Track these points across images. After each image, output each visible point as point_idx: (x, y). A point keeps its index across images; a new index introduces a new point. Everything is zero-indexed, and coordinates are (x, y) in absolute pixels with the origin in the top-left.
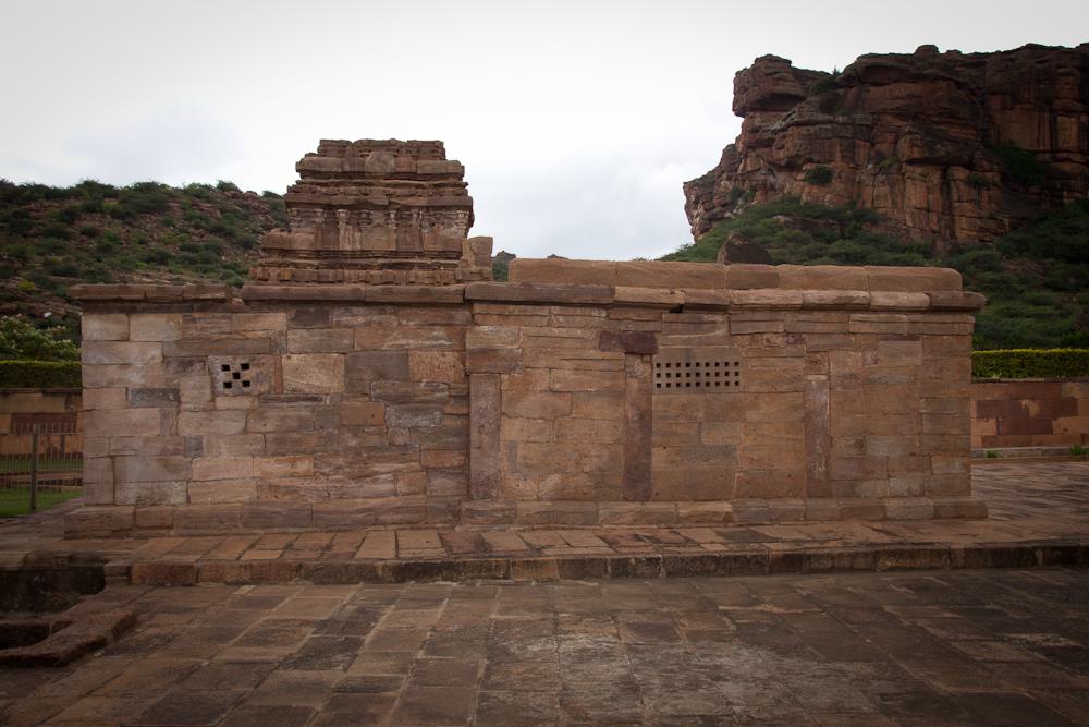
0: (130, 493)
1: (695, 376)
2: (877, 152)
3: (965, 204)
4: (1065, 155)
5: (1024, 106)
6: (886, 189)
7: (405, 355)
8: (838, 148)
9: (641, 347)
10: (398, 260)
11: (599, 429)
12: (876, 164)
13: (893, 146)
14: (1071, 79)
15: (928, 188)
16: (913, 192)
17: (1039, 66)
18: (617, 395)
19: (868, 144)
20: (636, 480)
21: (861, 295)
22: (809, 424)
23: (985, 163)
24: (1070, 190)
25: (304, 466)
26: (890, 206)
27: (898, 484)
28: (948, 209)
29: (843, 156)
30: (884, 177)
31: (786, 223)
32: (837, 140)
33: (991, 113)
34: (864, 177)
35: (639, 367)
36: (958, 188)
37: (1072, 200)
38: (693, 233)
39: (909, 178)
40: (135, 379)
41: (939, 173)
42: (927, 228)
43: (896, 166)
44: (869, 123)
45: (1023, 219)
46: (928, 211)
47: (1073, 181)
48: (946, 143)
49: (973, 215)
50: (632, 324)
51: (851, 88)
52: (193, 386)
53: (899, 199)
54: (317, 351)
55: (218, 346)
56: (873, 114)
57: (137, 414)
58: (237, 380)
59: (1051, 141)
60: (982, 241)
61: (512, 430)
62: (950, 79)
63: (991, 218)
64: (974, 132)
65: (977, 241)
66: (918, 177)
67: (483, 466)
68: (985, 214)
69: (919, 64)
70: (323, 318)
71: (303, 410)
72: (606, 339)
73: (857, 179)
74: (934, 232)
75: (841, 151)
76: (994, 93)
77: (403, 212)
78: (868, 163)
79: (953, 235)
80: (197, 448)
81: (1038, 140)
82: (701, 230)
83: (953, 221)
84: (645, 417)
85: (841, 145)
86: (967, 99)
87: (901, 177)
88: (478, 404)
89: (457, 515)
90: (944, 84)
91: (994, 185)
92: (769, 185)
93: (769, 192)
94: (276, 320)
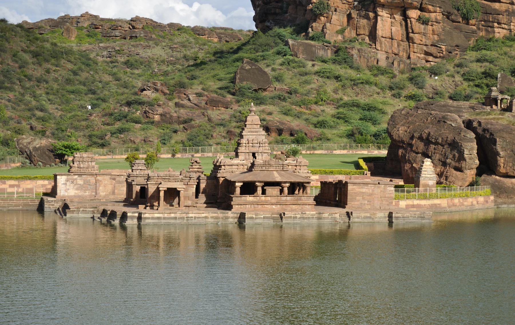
3: (416, 35)
9: (114, 179)
11: (110, 188)
16: (381, 25)
18: (112, 184)
20: (113, 193)
24: (499, 23)
31: (293, 45)
35: (114, 181)
37: (500, 30)
40: (62, 183)
45: (457, 46)
46: (392, 39)
49: (422, 43)
50: (113, 177)
52: (68, 183)
55: (71, 179)
57: (63, 186)
58: (72, 182)
60: (427, 61)
61: (101, 188)
67: (98, 192)
68: (429, 42)
72: (110, 179)
74: (395, 54)
79: (409, 57)
80: (68, 189)
82: (258, 19)
83: (409, 45)
84: (115, 187)
91: (437, 22)
92: (298, 3)
93: (299, 7)
94: (76, 176)
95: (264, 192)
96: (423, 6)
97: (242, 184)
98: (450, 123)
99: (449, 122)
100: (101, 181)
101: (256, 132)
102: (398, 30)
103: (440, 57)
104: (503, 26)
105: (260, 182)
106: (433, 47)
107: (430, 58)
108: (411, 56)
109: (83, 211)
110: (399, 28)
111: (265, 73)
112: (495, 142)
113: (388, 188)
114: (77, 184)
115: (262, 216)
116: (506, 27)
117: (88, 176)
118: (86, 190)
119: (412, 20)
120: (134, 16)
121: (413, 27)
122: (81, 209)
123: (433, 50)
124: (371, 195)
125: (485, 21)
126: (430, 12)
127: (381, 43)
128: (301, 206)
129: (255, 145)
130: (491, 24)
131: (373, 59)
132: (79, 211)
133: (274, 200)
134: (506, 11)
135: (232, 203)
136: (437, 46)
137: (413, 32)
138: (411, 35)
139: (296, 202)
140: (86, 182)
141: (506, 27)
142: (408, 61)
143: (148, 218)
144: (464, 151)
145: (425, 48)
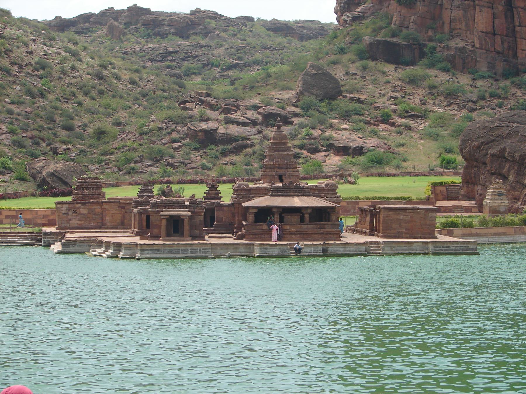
6: (459, 13)
7: (95, 209)
9: (123, 208)
10: (92, 195)
11: (118, 217)
15: (494, 14)
16: (480, 18)
18: (121, 213)
25: (83, 222)
26: (464, 28)
36: (518, 14)
38: (336, 12)
39: (478, 5)
40: (63, 212)
42: (493, 49)
46: (494, 34)
50: (122, 205)
52: (70, 213)
53: (471, 23)
58: (75, 212)
61: (108, 218)
70: (85, 205)
71: (83, 216)
72: (119, 207)
74: (498, 53)
79: (515, 56)
80: (70, 220)
83: (516, 41)
88: (104, 213)
94: (80, 205)
97: (255, 211)
108: (519, 54)
111: (335, 78)
113: (429, 214)
114: (80, 214)
120: (194, 9)
137: (520, 26)
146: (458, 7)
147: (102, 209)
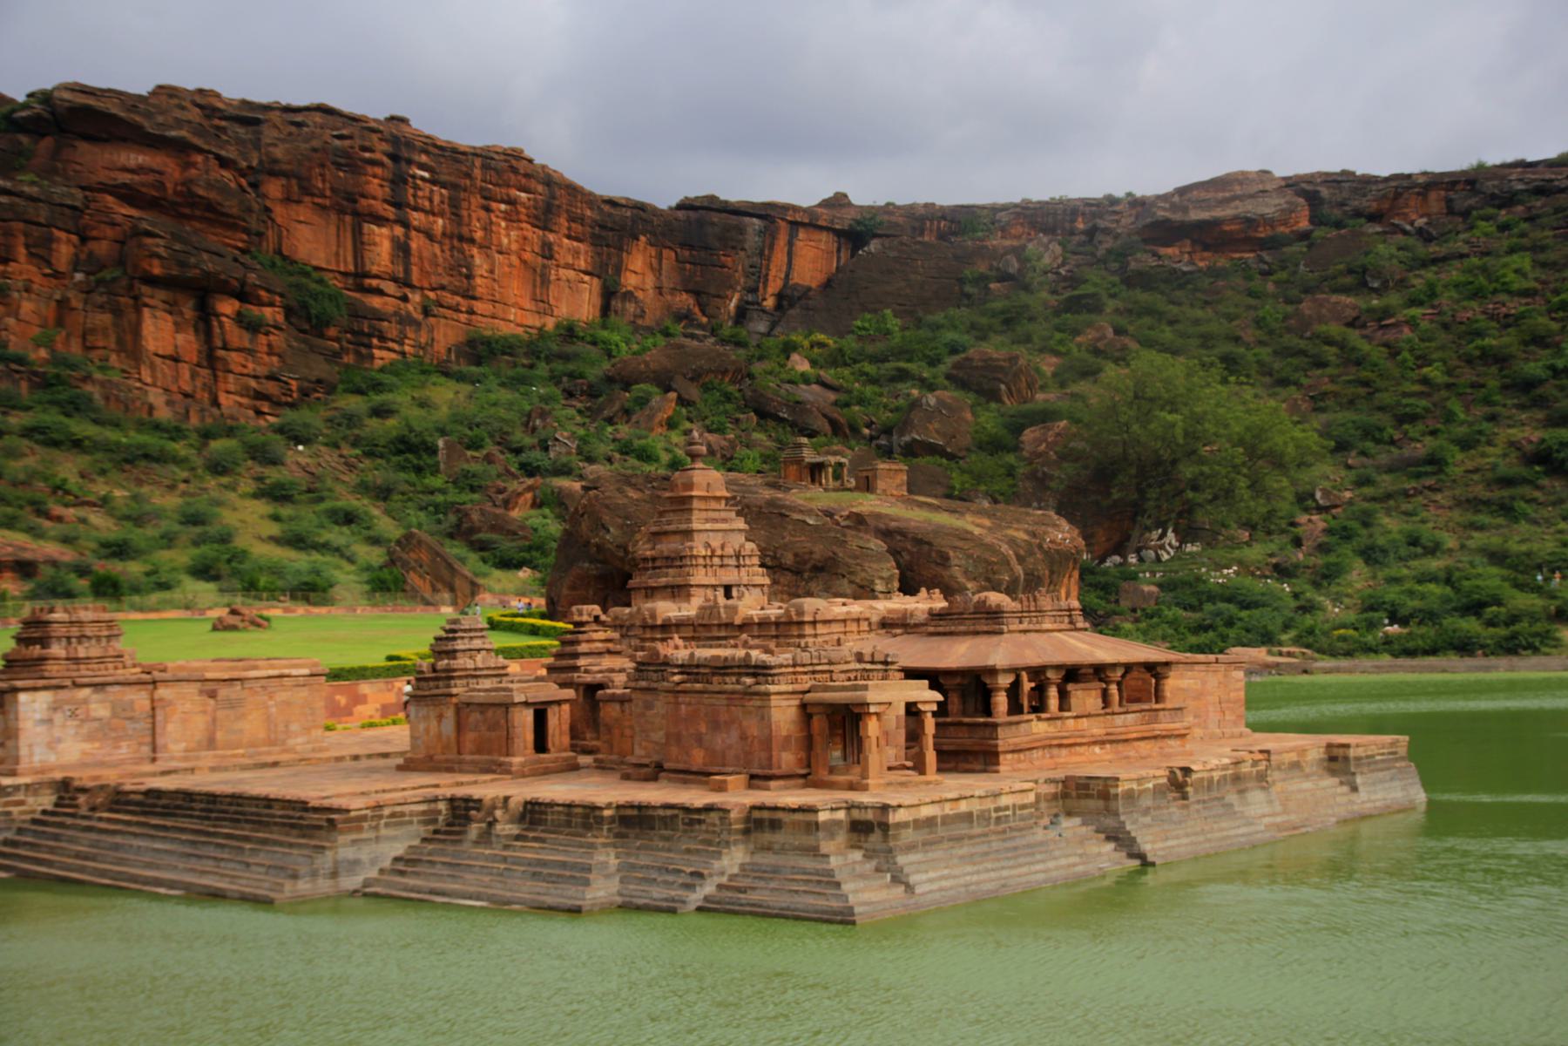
0: (36, 758)
1: (232, 705)
2: (91, 254)
3: (234, 354)
4: (374, 282)
5: (317, 200)
6: (106, 318)
7: (132, 702)
8: (22, 239)
9: (212, 695)
10: (101, 660)
11: (199, 723)
12: (88, 274)
13: (118, 246)
14: (378, 171)
16: (152, 328)
17: (337, 142)
18: (204, 712)
19: (74, 238)
20: (211, 743)
21: (286, 671)
22: (268, 719)
23: (263, 293)
24: (382, 338)
25: (97, 745)
26: (113, 346)
27: (300, 740)
28: (211, 359)
29: (31, 254)
30: (105, 298)
32: (21, 225)
33: (268, 203)
34: (71, 294)
35: (212, 702)
37: (384, 354)
40: (38, 716)
41: (191, 303)
43: (124, 283)
44: (78, 204)
45: (319, 381)
47: (386, 324)
48: (205, 256)
49: (245, 371)
51: (43, 136)
53: (129, 338)
54: (102, 702)
55: (68, 702)
56: (83, 188)
57: (39, 729)
58: (73, 715)
59: (355, 258)
61: (170, 727)
62: (209, 152)
63: (272, 377)
64: (245, 237)
65: (251, 413)
66: (161, 305)
67: (160, 741)
68: (262, 370)
69: (160, 119)
71: (96, 724)
72: (201, 692)
73: (58, 297)
74: (186, 395)
75: (27, 246)
76: (273, 174)
77: (98, 638)
78: (76, 270)
79: (215, 403)
80: (59, 740)
81: (337, 254)
83: (215, 376)
84: (214, 720)
85: (26, 235)
86: (233, 185)
87: (131, 302)
88: (159, 718)
89: (154, 760)
90: (199, 158)
91: (276, 327)
94: (87, 692)
95: (1064, 704)
96: (247, 289)
98: (800, 517)
99: (796, 516)
100: (170, 703)
101: (725, 520)
102: (187, 342)
103: (287, 404)
104: (391, 345)
105: (1058, 667)
106: (272, 383)
107: (265, 408)
109: (393, 815)
110: (192, 338)
112: (944, 560)
114: (88, 719)
115: (1150, 785)
116: (396, 346)
117: (127, 689)
118: (118, 739)
119: (224, 319)
121: (228, 337)
122: (387, 812)
123: (272, 388)
124: (1199, 695)
125: (353, 332)
126: (261, 304)
127: (152, 367)
128: (1160, 743)
129: (726, 561)
130: (365, 340)
131: (138, 404)
132: (381, 817)
133: (1096, 728)
134: (396, 314)
135: (1002, 745)
136: (278, 380)
137: (225, 348)
138: (221, 353)
139: (1145, 729)
140: (122, 712)
141: (396, 346)
142: (215, 411)
143: (905, 825)
144: (872, 582)
145: (253, 383)
146: (101, 307)
147: (153, 701)
